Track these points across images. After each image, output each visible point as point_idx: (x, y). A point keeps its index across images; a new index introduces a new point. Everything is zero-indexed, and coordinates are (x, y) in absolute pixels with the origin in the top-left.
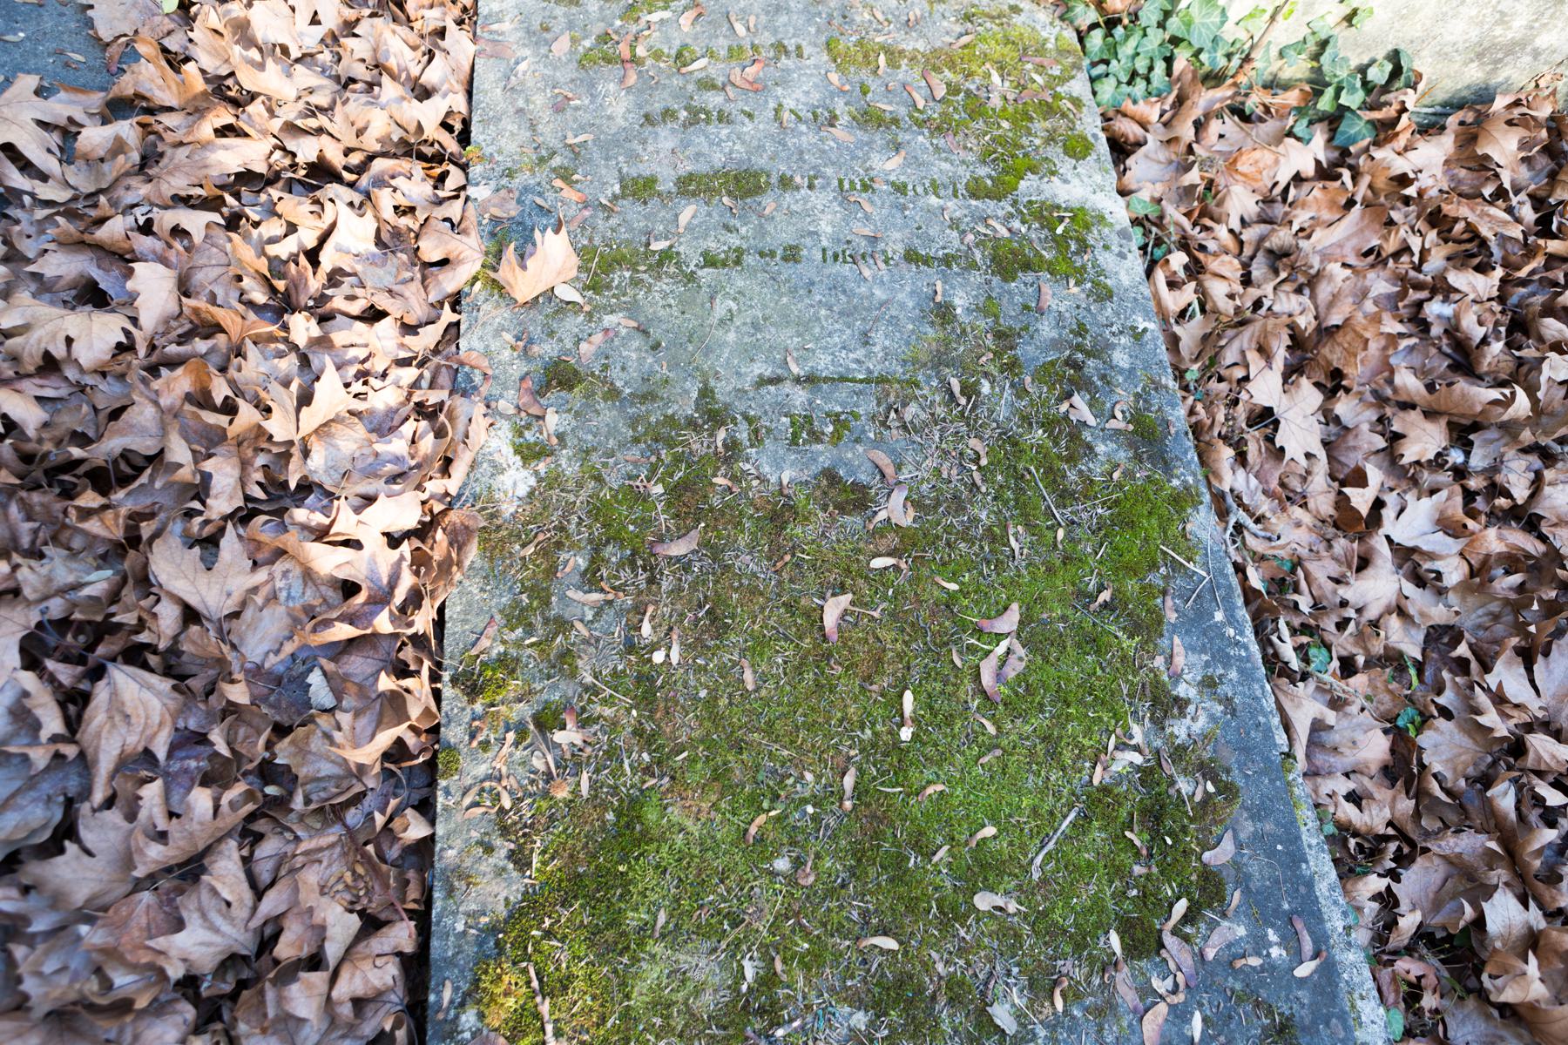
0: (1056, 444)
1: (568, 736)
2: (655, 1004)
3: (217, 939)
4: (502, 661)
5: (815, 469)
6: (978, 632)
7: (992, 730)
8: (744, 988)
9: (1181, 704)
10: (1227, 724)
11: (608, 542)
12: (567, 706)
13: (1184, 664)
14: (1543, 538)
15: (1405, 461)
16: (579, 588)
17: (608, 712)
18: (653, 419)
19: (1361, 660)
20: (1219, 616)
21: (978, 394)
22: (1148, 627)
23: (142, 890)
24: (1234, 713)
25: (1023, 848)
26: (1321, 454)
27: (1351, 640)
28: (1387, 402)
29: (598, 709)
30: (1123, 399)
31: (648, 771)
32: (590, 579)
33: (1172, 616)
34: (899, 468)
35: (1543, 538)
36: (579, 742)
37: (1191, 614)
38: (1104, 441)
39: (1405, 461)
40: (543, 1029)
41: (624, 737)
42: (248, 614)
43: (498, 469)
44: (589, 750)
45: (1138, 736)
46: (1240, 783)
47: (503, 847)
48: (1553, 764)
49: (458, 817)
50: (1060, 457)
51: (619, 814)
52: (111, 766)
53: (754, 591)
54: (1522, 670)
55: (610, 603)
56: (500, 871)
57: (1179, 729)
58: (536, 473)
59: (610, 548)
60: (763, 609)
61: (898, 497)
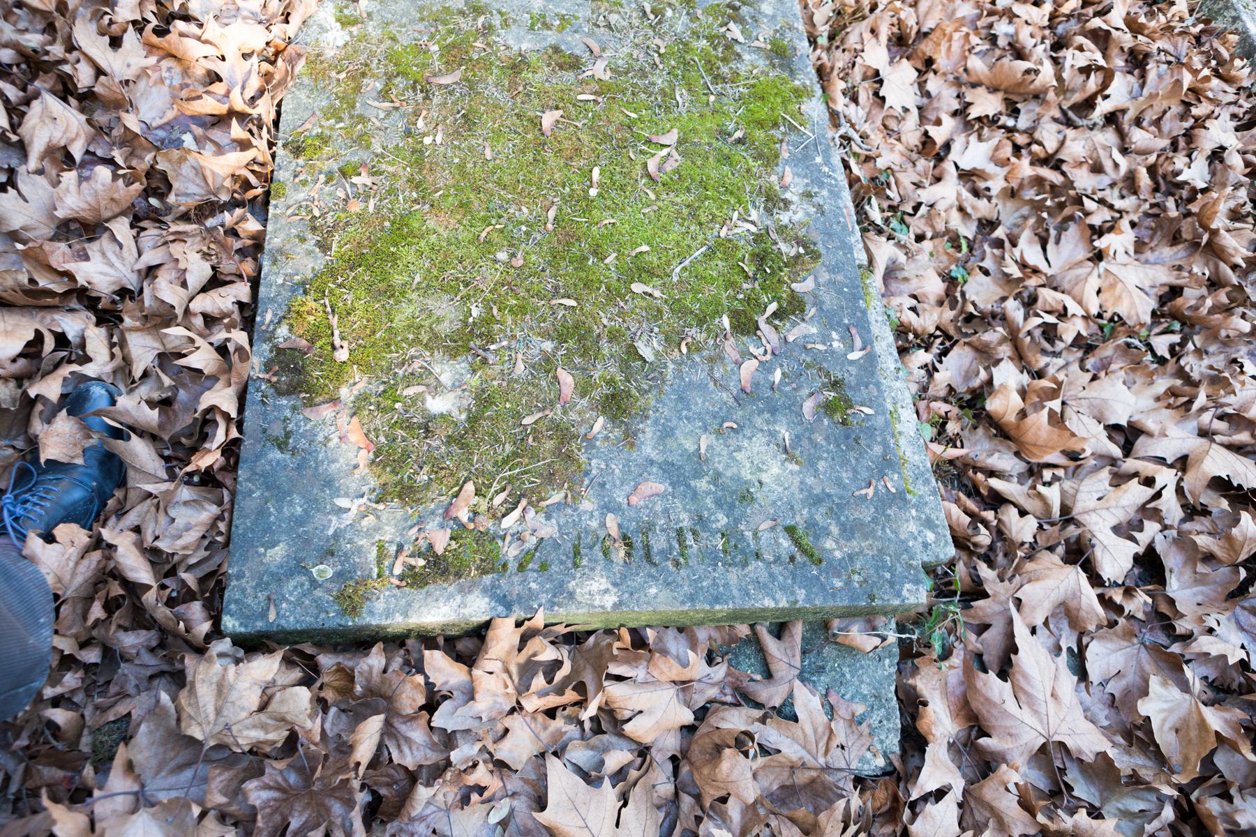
0: (715, 49)
1: (363, 180)
2: (409, 326)
3: (112, 271)
4: (320, 136)
5: (544, 44)
6: (648, 142)
7: (652, 196)
8: (471, 320)
9: (787, 204)
10: (818, 219)
11: (398, 75)
12: (363, 164)
13: (792, 182)
14: (1063, 174)
15: (970, 117)
16: (375, 99)
17: (391, 169)
18: (434, 9)
19: (929, 234)
20: (819, 160)
21: (663, 16)
22: (770, 160)
23: (59, 240)
24: (823, 213)
25: (668, 263)
26: (915, 112)
27: (923, 221)
28: (963, 82)
29: (384, 167)
30: (765, 33)
31: (415, 201)
32: (384, 95)
33: (786, 155)
34: (603, 50)
35: (1063, 174)
36: (369, 184)
37: (800, 156)
38: (749, 53)
39: (970, 117)
40: (332, 334)
41: (400, 184)
42: (142, 84)
43: (323, 30)
44: (375, 187)
45: (754, 215)
46: (823, 251)
47: (312, 239)
48: (1054, 304)
49: (283, 221)
50: (717, 57)
51: (393, 223)
52: (42, 149)
53: (497, 107)
54: (1039, 248)
55: (397, 109)
56: (309, 253)
57: (784, 218)
58: (351, 32)
59: (399, 79)
60: (501, 116)
61: (601, 65)
